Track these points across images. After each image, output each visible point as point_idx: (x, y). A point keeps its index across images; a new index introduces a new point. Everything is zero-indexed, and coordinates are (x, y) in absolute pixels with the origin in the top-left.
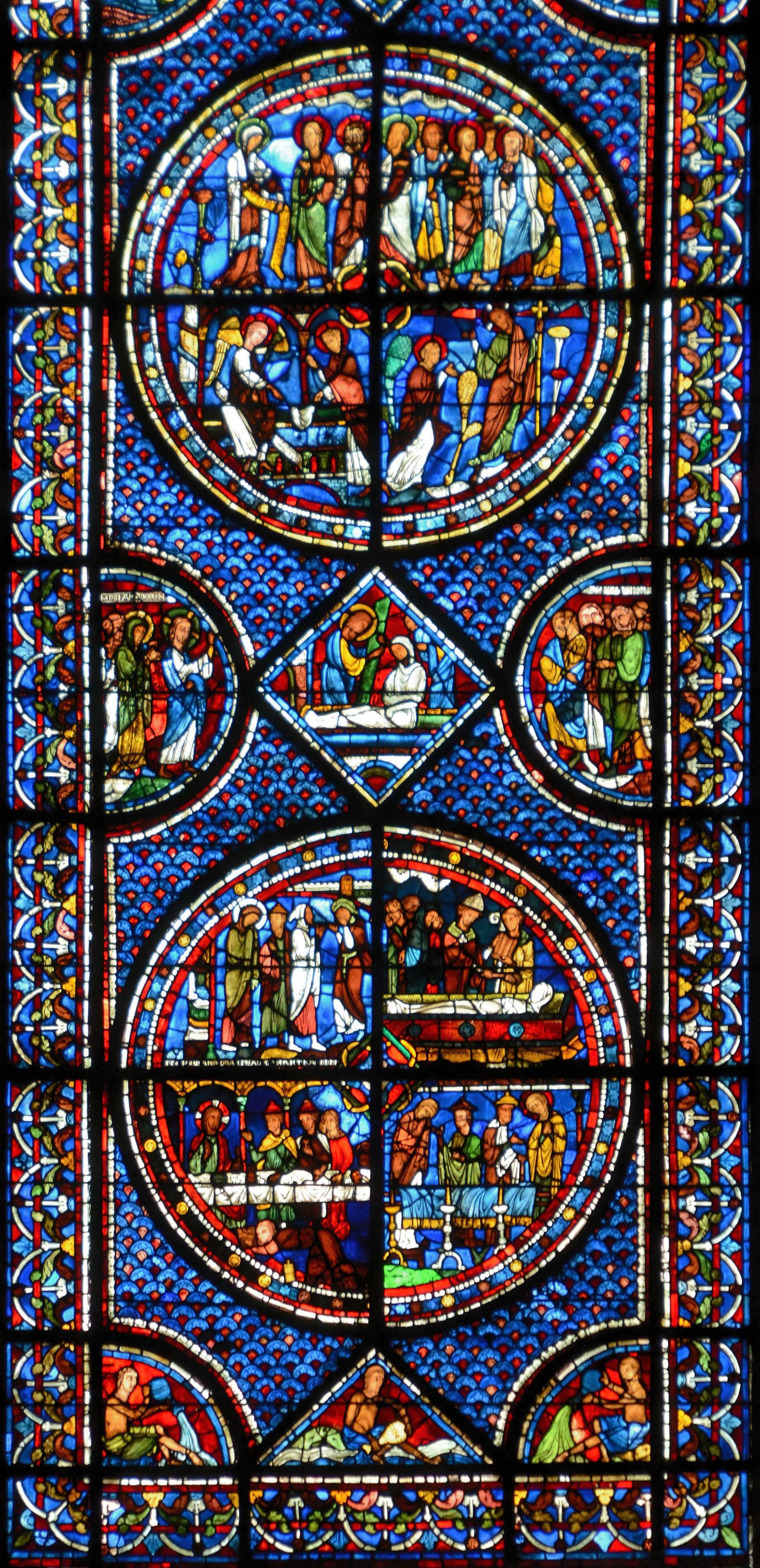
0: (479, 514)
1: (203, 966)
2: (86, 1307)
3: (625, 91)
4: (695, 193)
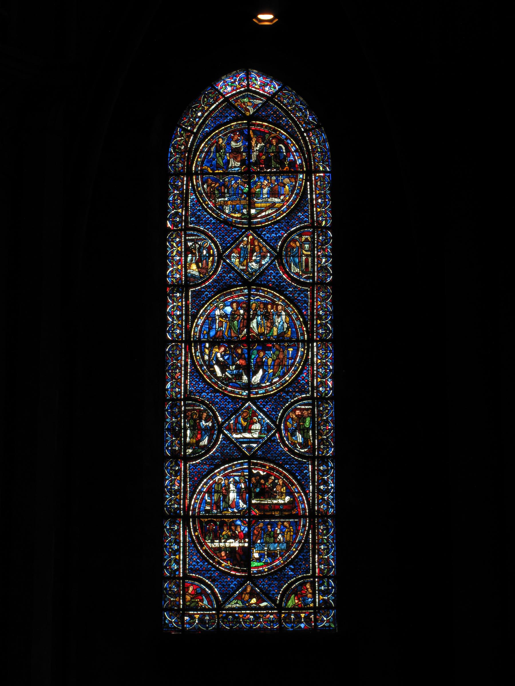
0: (273, 390)
1: (210, 492)
2: (181, 571)
3: (305, 297)
4: (321, 319)
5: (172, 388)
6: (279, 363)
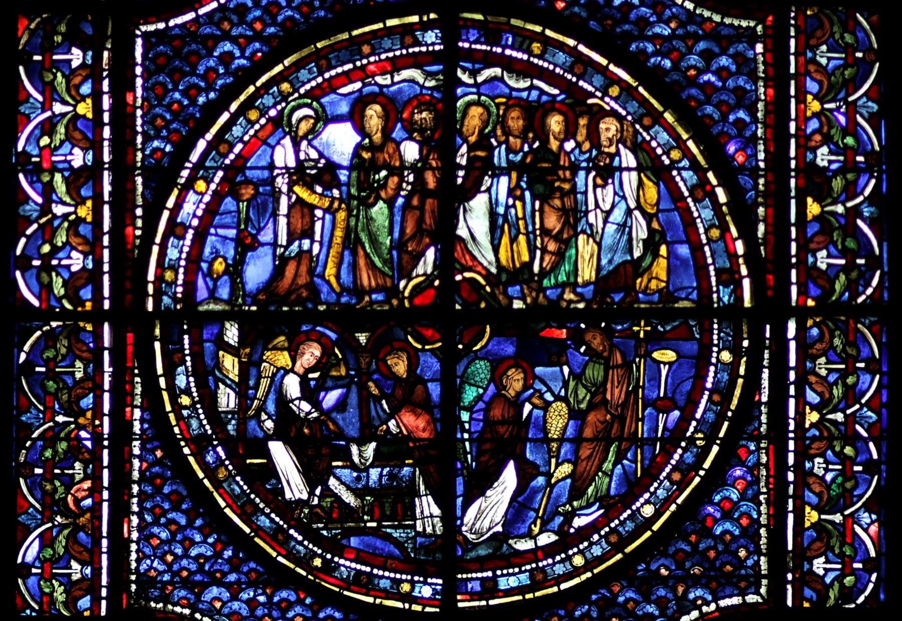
0: (572, 570)
5: (50, 564)
6: (606, 429)
